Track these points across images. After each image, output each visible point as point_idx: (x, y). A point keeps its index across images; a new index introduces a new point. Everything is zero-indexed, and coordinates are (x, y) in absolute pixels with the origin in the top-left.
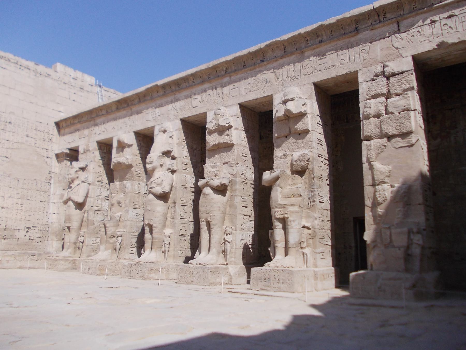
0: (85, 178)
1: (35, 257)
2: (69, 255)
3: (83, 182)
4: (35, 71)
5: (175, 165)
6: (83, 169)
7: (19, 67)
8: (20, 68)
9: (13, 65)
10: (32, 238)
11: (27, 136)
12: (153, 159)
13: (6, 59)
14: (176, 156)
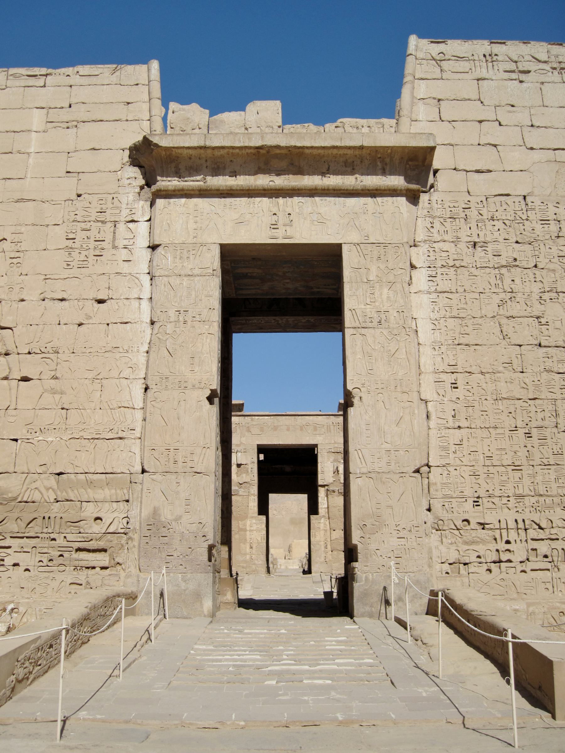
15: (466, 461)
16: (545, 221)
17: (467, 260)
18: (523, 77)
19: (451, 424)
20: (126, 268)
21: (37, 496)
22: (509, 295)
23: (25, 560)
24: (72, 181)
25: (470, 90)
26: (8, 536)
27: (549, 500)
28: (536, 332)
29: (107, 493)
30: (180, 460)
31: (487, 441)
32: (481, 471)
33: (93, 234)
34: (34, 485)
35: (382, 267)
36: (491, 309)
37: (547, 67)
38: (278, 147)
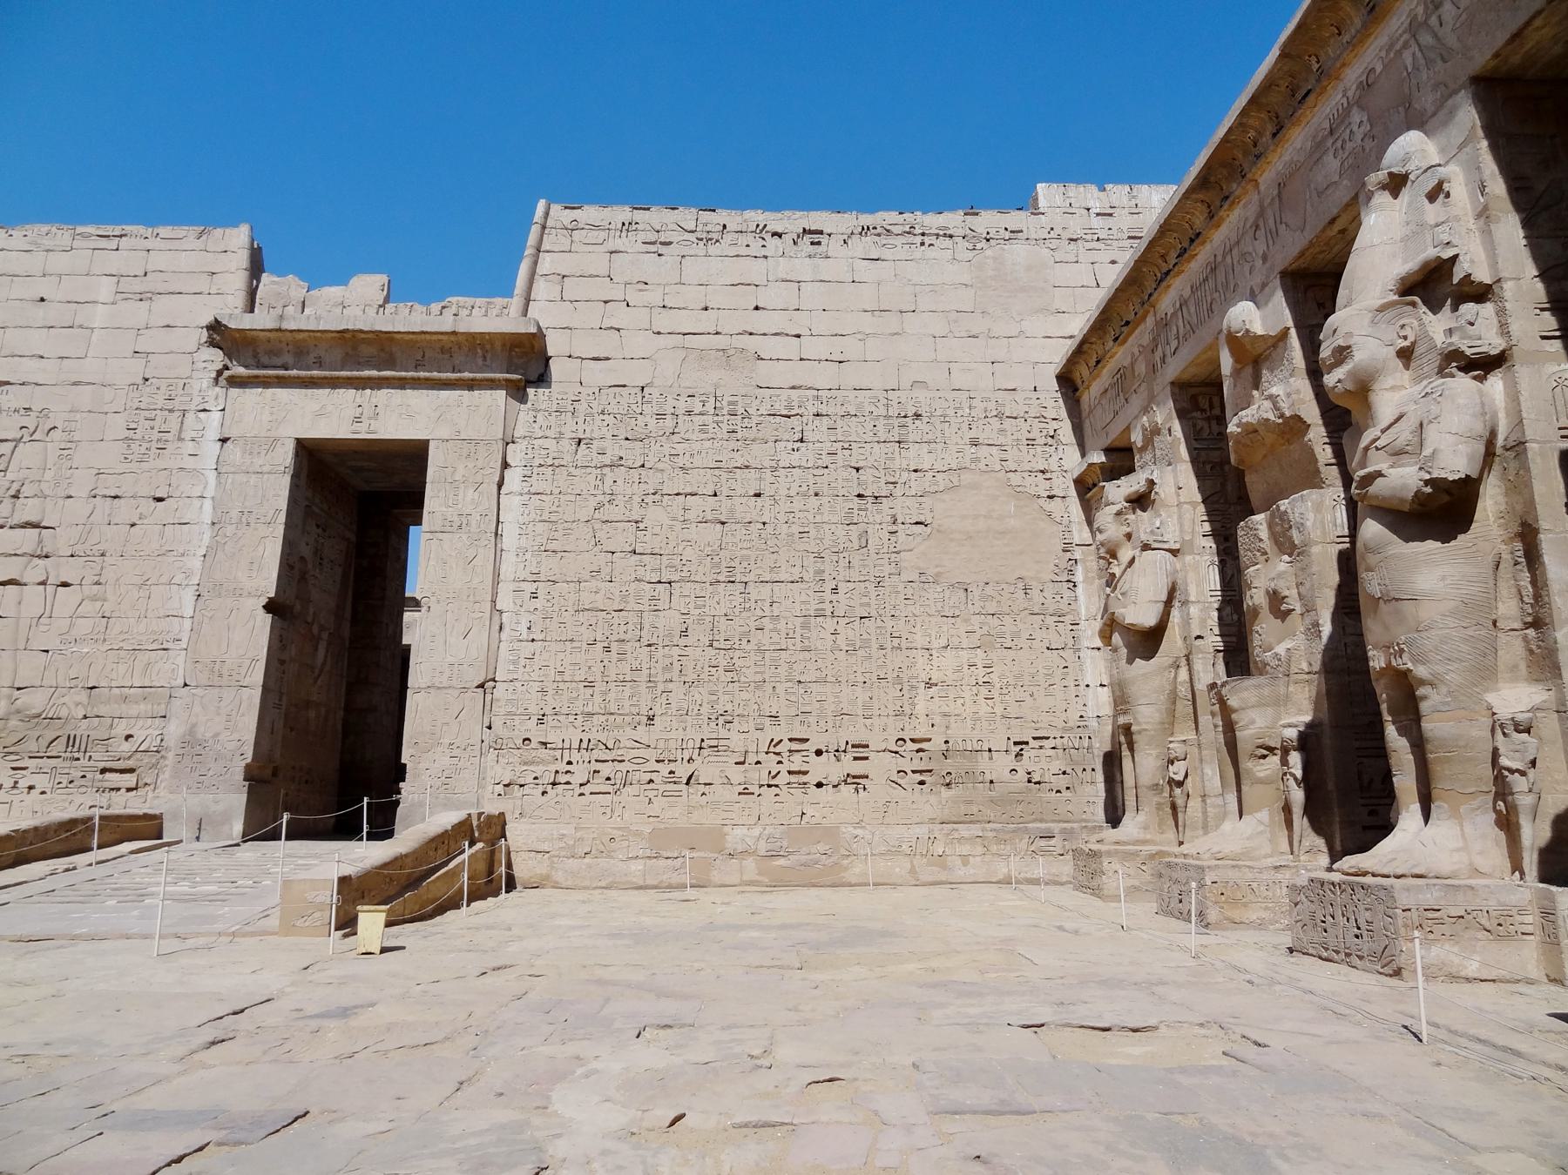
0: (1152, 532)
1: (1053, 842)
2: (1142, 836)
3: (1146, 547)
4: (969, 236)
5: (1479, 328)
6: (1141, 501)
7: (919, 239)
8: (922, 244)
9: (900, 240)
10: (1036, 778)
11: (975, 443)
12: (1349, 334)
13: (879, 230)
14: (1483, 275)
15: (534, 676)
16: (660, 416)
17: (567, 459)
18: (662, 249)
19: (525, 636)
20: (190, 463)
21: (64, 713)
22: (608, 498)
23: (41, 782)
24: (139, 363)
25: (599, 263)
26: (26, 755)
27: (619, 719)
28: (631, 539)
29: (143, 707)
30: (225, 673)
31: (561, 656)
32: (550, 687)
33: (157, 424)
34: (63, 700)
35: (471, 465)
36: (584, 515)
37: (692, 237)
38: (361, 331)
